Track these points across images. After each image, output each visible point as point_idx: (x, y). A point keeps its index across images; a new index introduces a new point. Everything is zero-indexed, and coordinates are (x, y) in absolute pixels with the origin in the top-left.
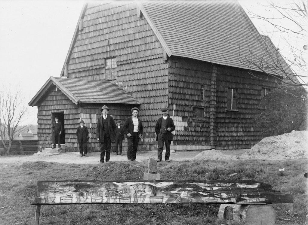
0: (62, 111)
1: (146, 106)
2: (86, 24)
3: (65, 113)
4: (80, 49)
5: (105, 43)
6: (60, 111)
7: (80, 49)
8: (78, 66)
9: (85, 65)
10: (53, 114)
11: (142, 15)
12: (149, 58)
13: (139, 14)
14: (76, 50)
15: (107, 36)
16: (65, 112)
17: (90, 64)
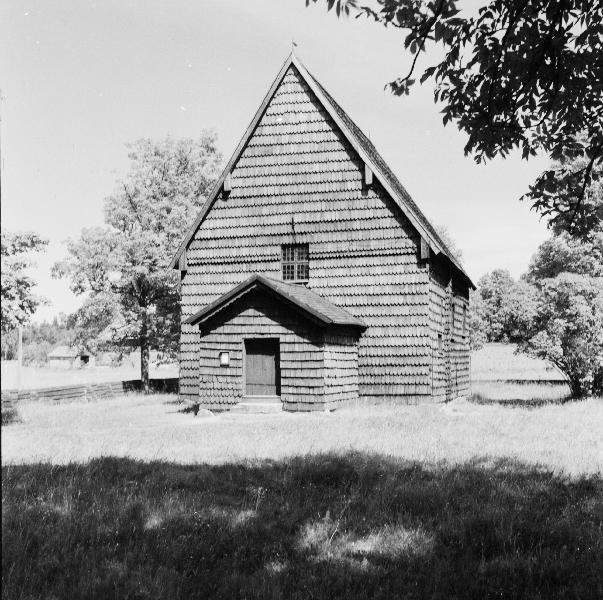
0: (277, 336)
1: (379, 332)
2: (240, 182)
3: (281, 340)
4: (219, 223)
5: (287, 219)
6: (269, 336)
7: (219, 223)
8: (210, 254)
9: (234, 252)
10: (248, 342)
11: (374, 177)
12: (388, 252)
13: (369, 181)
14: (205, 224)
15: (289, 208)
16: (282, 339)
17: (245, 252)
